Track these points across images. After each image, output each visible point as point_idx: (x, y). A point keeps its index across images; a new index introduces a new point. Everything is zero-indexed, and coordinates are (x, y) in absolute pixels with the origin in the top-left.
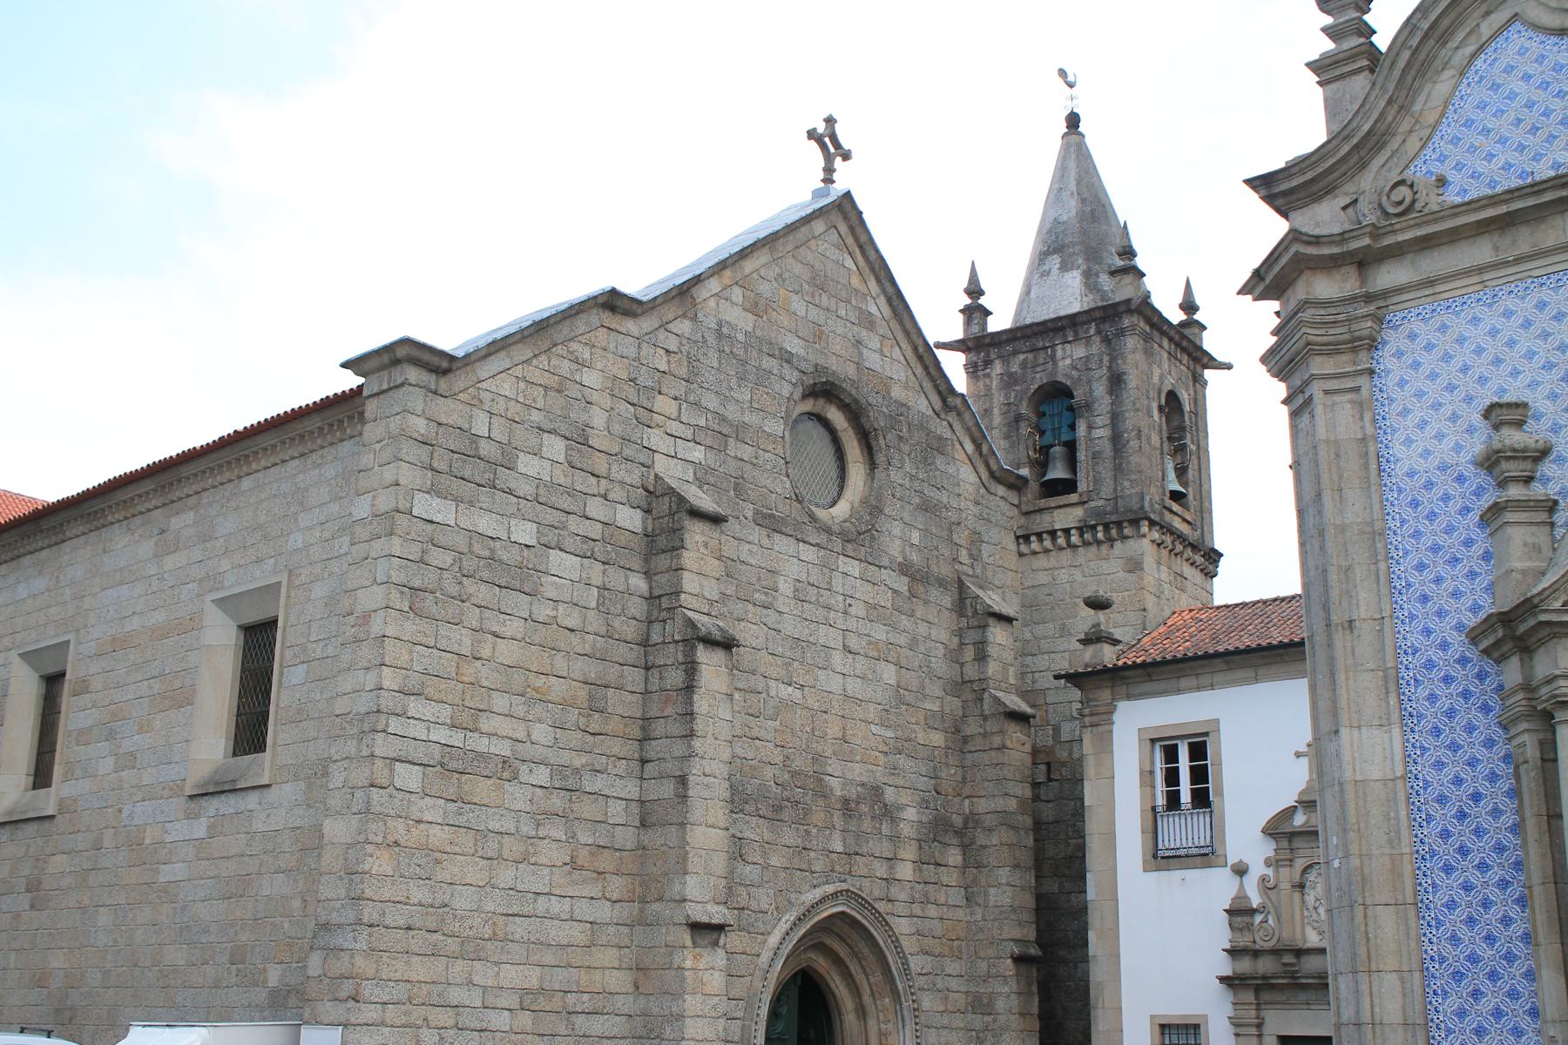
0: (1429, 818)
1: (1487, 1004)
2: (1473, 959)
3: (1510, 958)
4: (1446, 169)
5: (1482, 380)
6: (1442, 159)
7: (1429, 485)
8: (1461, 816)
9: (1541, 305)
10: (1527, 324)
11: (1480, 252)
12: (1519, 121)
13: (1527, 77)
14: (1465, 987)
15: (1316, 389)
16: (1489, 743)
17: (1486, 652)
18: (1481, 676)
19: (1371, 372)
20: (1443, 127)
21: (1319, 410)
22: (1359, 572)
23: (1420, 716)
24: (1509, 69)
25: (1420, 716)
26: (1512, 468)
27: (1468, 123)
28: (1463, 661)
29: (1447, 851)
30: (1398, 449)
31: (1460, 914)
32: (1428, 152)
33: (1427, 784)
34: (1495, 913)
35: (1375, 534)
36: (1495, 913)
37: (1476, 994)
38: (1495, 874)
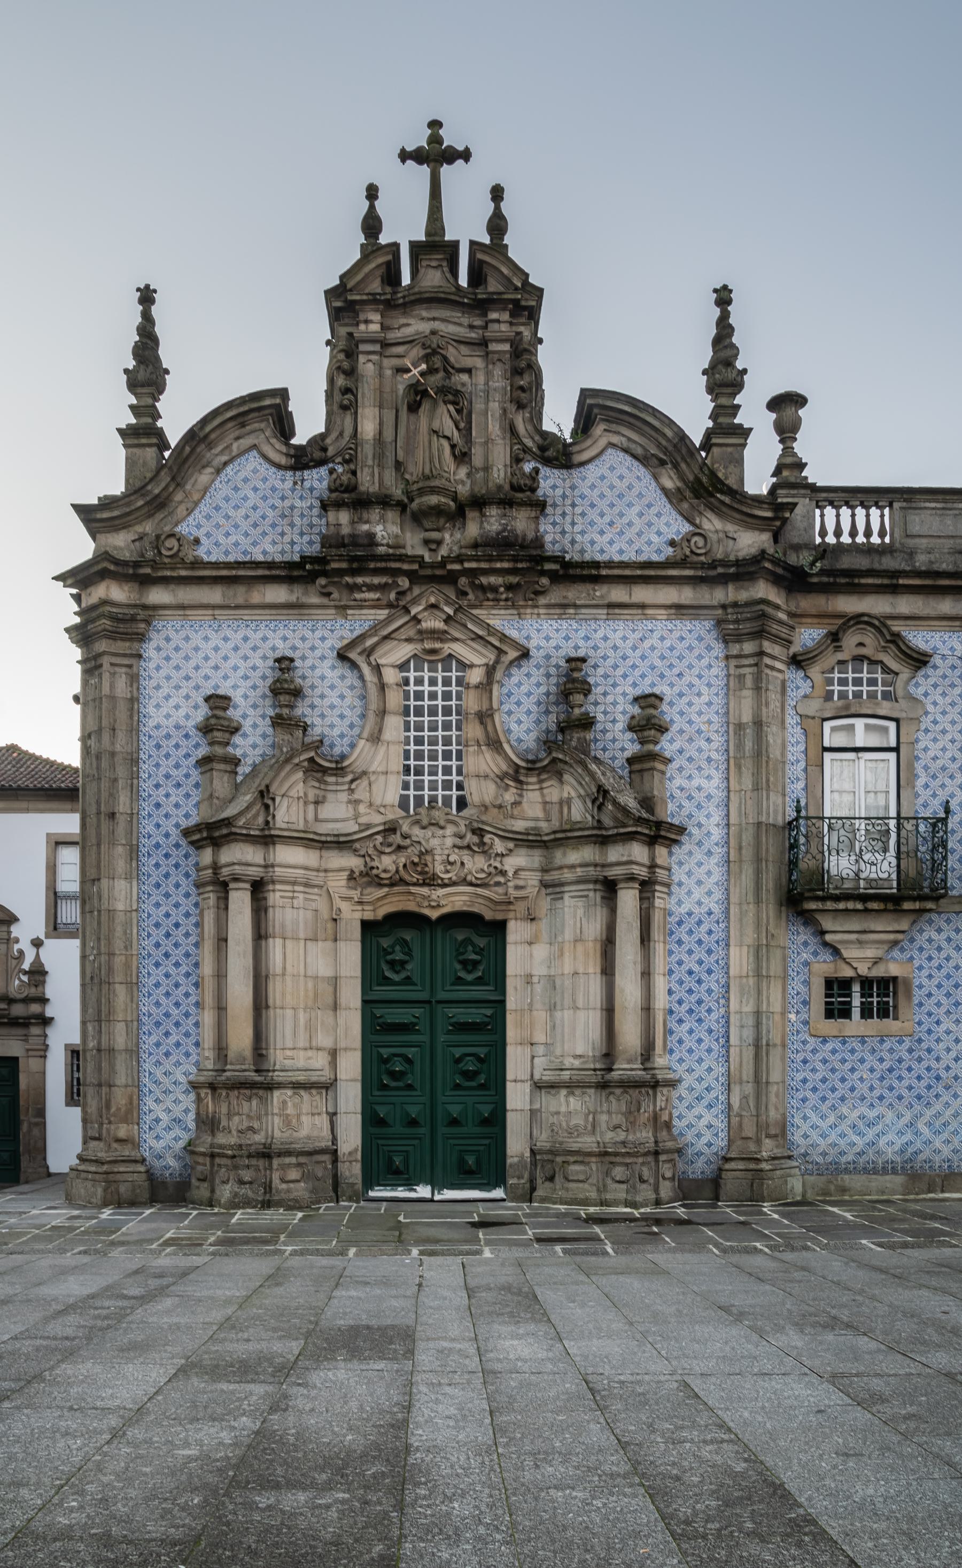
0: (149, 935)
1: (172, 1039)
2: (167, 1015)
3: (187, 1015)
4: (200, 534)
5: (207, 678)
6: (199, 526)
7: (168, 737)
8: (168, 935)
9: (246, 639)
10: (236, 649)
11: (214, 595)
12: (247, 517)
13: (255, 489)
14: (162, 1030)
15: (106, 661)
16: (187, 895)
17: (192, 843)
18: (187, 856)
19: (140, 656)
20: (202, 505)
21: (106, 676)
22: (121, 783)
23: (149, 876)
24: (246, 480)
25: (149, 876)
26: (218, 735)
27: (217, 508)
28: (177, 846)
29: (158, 954)
30: (151, 710)
31: (162, 990)
32: (190, 519)
33: (149, 915)
34: (182, 990)
35: (134, 761)
36: (182, 990)
37: (167, 1034)
38: (183, 969)
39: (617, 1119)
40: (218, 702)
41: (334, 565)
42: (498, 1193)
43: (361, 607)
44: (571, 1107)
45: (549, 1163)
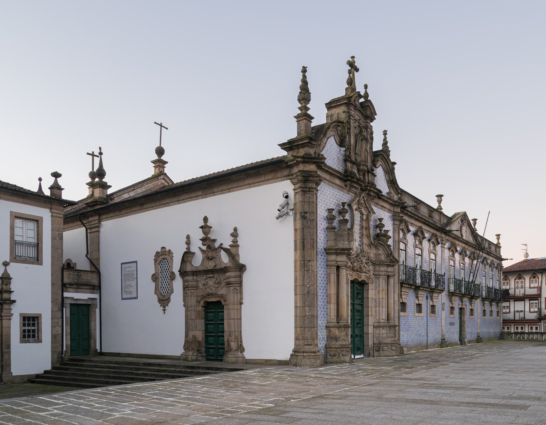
38: (325, 291)
39: (392, 335)
40: (330, 211)
41: (355, 180)
42: (362, 356)
43: (351, 192)
44: (383, 332)
45: (378, 347)
